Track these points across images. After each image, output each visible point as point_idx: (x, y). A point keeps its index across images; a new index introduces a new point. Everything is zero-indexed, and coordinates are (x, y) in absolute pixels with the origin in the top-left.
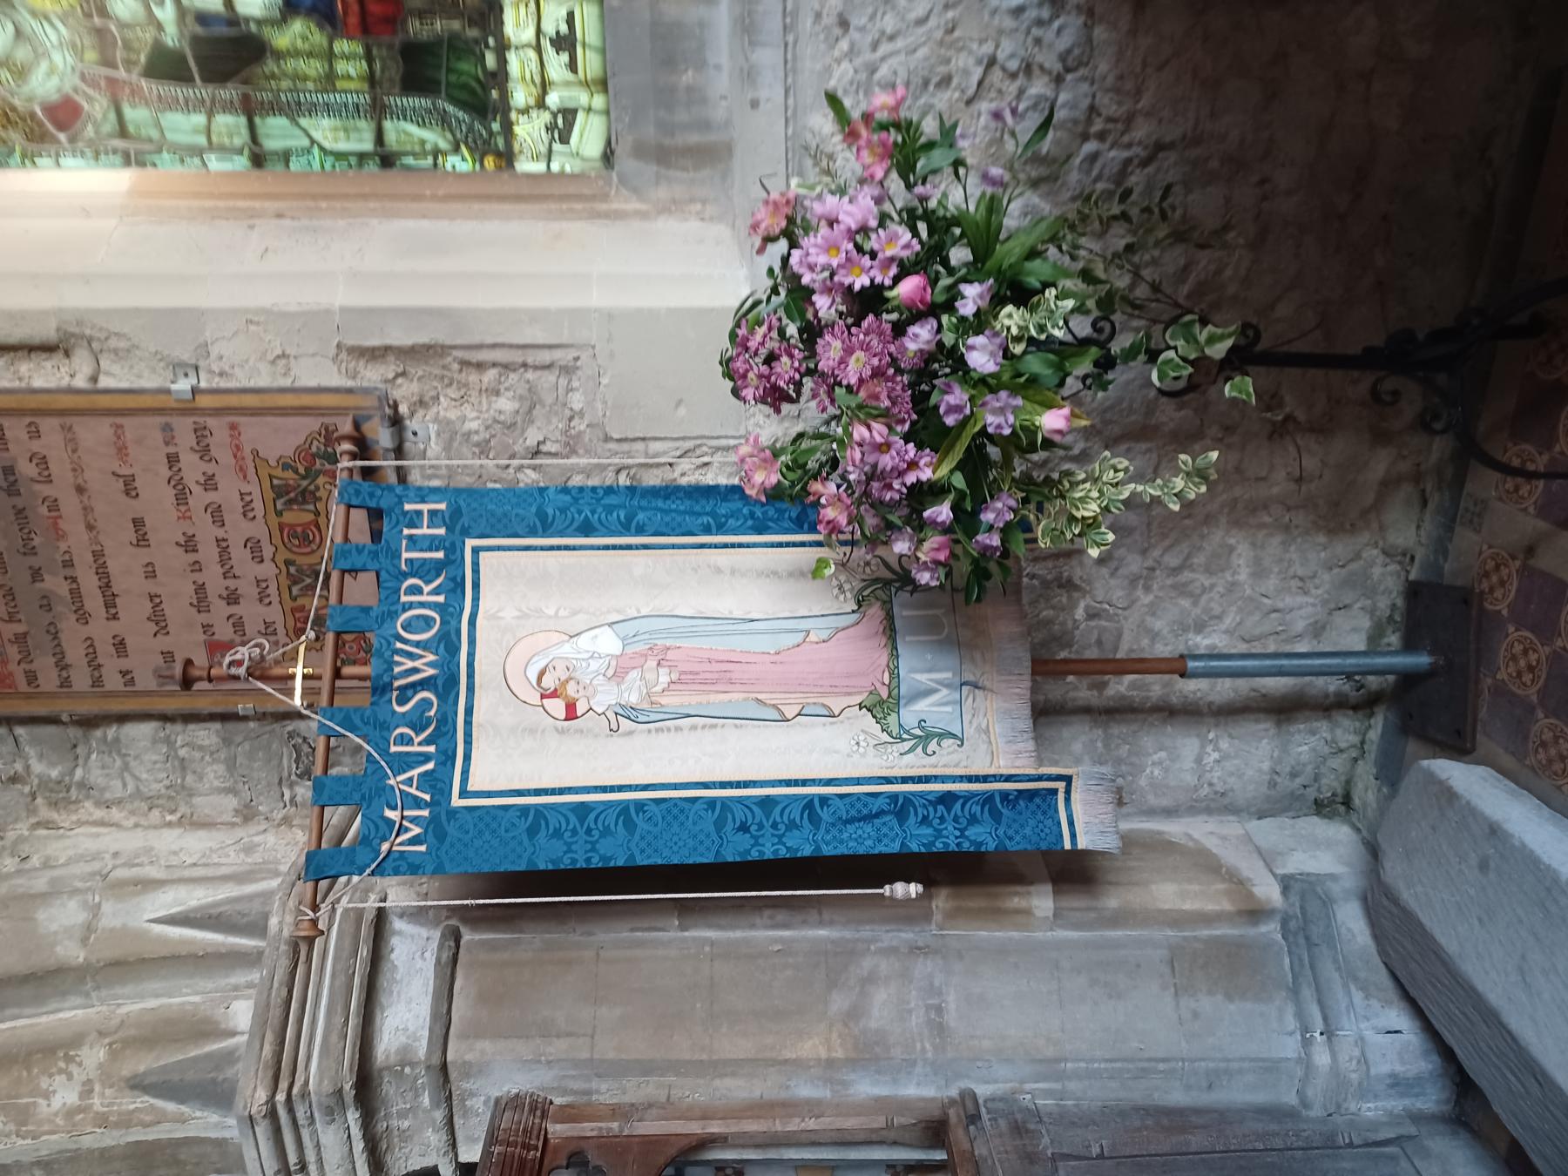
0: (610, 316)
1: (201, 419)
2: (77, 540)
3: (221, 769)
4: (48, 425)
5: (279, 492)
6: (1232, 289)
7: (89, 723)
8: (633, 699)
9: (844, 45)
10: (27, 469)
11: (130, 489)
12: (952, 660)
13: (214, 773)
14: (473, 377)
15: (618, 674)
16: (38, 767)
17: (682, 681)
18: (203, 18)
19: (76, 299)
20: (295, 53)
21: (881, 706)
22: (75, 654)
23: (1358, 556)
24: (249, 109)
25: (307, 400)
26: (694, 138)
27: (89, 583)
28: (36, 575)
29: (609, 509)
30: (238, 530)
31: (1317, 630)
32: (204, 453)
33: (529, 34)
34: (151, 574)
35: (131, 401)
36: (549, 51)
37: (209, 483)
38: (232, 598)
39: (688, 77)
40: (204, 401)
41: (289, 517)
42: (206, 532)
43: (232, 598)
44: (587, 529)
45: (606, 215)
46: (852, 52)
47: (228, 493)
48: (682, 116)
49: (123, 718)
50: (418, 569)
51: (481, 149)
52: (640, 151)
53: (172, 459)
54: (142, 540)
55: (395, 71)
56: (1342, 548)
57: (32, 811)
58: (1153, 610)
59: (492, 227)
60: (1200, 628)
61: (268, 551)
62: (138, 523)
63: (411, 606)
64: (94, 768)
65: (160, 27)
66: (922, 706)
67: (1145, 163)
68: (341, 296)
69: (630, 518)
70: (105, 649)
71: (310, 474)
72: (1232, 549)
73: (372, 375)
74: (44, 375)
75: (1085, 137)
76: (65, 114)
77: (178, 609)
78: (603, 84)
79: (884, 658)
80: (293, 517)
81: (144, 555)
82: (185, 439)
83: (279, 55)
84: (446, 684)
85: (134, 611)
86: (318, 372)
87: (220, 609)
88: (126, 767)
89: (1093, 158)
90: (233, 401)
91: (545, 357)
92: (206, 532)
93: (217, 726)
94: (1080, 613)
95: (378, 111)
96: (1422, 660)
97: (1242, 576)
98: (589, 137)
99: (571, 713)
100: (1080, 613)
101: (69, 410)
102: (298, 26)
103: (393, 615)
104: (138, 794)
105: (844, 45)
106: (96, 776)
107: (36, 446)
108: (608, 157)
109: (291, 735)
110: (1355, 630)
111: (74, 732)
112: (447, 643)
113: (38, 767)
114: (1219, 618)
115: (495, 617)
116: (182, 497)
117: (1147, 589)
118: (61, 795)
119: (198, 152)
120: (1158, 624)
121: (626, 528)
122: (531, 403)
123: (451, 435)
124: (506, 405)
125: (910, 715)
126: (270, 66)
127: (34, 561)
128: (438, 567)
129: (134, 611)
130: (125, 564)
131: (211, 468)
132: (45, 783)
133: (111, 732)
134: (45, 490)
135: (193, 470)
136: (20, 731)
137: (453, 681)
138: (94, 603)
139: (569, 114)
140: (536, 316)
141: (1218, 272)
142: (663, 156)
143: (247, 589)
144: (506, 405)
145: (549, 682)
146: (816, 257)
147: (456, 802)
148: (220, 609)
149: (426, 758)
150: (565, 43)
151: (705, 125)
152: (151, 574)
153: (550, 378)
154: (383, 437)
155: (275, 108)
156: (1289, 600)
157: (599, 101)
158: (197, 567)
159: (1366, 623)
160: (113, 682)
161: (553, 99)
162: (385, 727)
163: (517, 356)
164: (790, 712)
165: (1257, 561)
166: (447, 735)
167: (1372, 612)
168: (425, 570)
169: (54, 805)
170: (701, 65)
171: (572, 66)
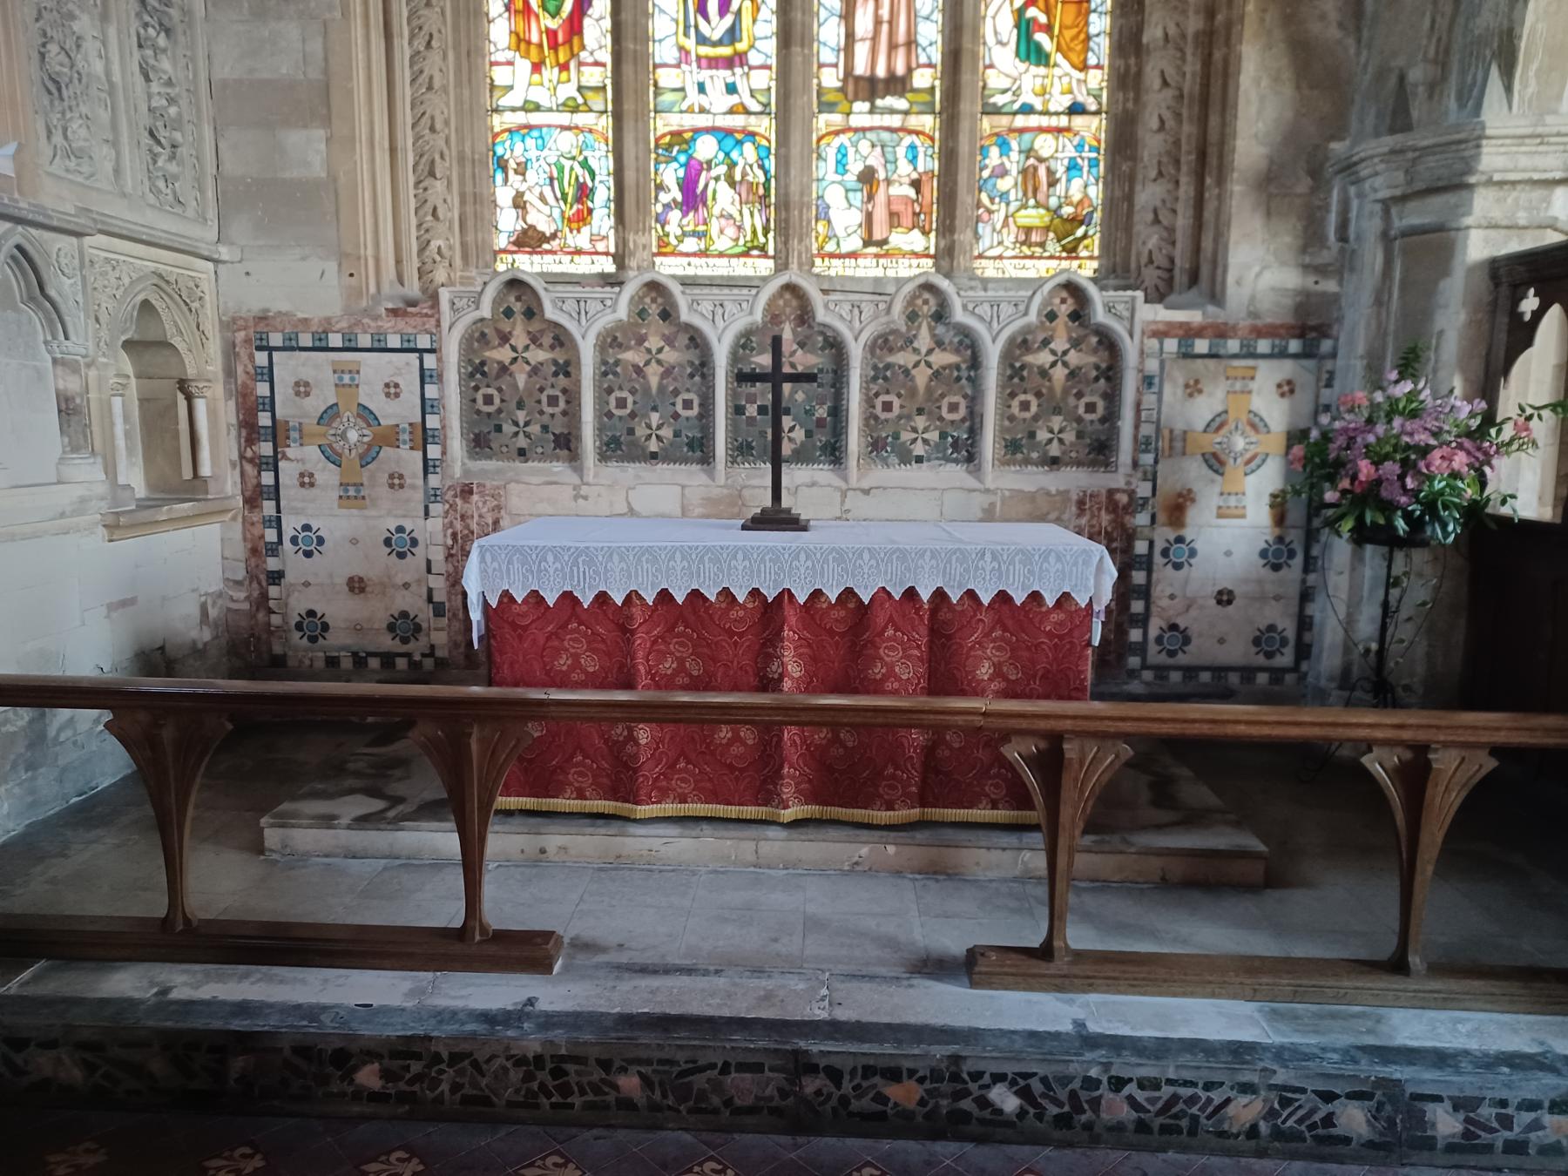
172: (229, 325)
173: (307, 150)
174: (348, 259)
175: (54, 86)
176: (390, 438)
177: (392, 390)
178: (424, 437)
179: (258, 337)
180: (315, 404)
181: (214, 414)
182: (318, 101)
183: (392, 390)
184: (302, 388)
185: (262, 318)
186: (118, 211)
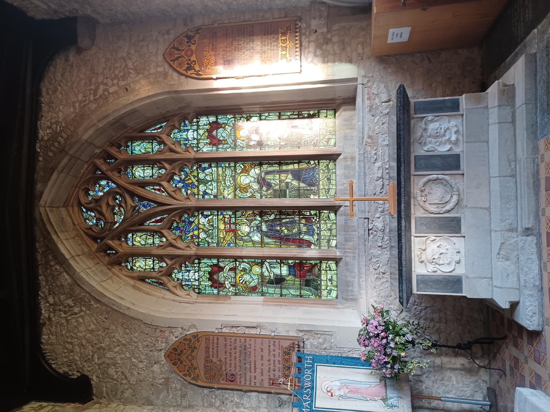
0: (338, 327)
1: (275, 339)
2: (252, 359)
3: (266, 403)
4: (253, 339)
5: (285, 352)
6: (443, 330)
7: (246, 392)
8: (342, 394)
9: (375, 290)
10: (248, 346)
11: (262, 351)
12: (396, 392)
13: (264, 404)
14: (316, 336)
15: (340, 389)
16: (236, 399)
17: (351, 391)
18: (277, 275)
19: (260, 320)
20: (290, 281)
21: (384, 400)
22: (248, 379)
23: (477, 381)
24: (281, 288)
25: (291, 338)
26: (351, 297)
27: (253, 366)
28: (245, 364)
29: (338, 360)
30: (277, 358)
31: (472, 396)
32: (274, 345)
33: (325, 279)
34: (262, 365)
35: (265, 336)
36: (328, 281)
37: (274, 350)
38: (274, 371)
39: (351, 288)
40: (276, 337)
41: (285, 357)
42: (272, 358)
43: (274, 371)
44: (334, 363)
45: (337, 308)
46: (376, 292)
47: (276, 353)
48: (349, 294)
49: (252, 391)
50: (307, 368)
51: (316, 296)
52: (343, 298)
53: (269, 346)
54: (262, 359)
55: (304, 283)
56: (473, 379)
57: (233, 408)
58: (438, 388)
59: (318, 309)
60: (448, 393)
61: (281, 362)
62: (262, 356)
63: (306, 374)
64: (245, 401)
65: (270, 276)
66: (391, 400)
67: (425, 310)
68: (298, 322)
69: (341, 362)
70: (253, 378)
71: (290, 350)
72: (451, 377)
73: (301, 334)
74: (253, 331)
75: (414, 305)
76: (254, 289)
77: (265, 372)
78: (337, 286)
79: (384, 391)
80: (286, 357)
81: (262, 362)
82: (272, 343)
83: (287, 281)
84: (312, 388)
85: (259, 371)
86: (293, 334)
87: (272, 372)
88: (250, 401)
89: (416, 308)
90: (280, 337)
91: (328, 333)
92: (272, 358)
93: (266, 394)
94: (424, 387)
95: (301, 289)
96: (489, 403)
97: (455, 383)
98: (334, 294)
99: (332, 396)
100: (424, 387)
102: (290, 277)
103: (304, 375)
104: (251, 407)
105: (375, 290)
106: (245, 403)
107: (250, 343)
108: (337, 297)
109: (279, 398)
110: (480, 397)
111: (243, 393)
112: (312, 381)
113: (236, 399)
114: (451, 391)
115: (319, 377)
116: (269, 353)
117: (436, 384)
118: (238, 405)
119: (273, 294)
120: (440, 391)
121: (341, 364)
122: (325, 340)
123: (312, 344)
124: (321, 340)
125: (389, 402)
126: (285, 282)
127: (245, 361)
128: (311, 368)
129: (259, 371)
130: (259, 363)
131: (275, 348)
132: (236, 402)
133: (249, 394)
134: (250, 350)
135: (272, 347)
136: (235, 392)
137: (313, 388)
138: (253, 370)
139: (331, 290)
140: (327, 327)
141: (440, 327)
142: (346, 300)
143: (277, 369)
144: (321, 340)
145: (329, 390)
146: (370, 328)
147: (314, 409)
148: (272, 372)
149: (309, 401)
150: (331, 280)
151: (353, 295)
152: (262, 365)
153: (328, 336)
154: (302, 345)
155: (286, 288)
156: (465, 389)
157: (336, 289)
158: (270, 364)
159: (482, 395)
160: (253, 384)
161: (328, 288)
162: (303, 395)
163: (323, 333)
164: (369, 399)
165: (457, 380)
166: (312, 397)
167: (483, 393)
168: (308, 368)
169: (236, 407)
170: (353, 287)
171: (332, 283)
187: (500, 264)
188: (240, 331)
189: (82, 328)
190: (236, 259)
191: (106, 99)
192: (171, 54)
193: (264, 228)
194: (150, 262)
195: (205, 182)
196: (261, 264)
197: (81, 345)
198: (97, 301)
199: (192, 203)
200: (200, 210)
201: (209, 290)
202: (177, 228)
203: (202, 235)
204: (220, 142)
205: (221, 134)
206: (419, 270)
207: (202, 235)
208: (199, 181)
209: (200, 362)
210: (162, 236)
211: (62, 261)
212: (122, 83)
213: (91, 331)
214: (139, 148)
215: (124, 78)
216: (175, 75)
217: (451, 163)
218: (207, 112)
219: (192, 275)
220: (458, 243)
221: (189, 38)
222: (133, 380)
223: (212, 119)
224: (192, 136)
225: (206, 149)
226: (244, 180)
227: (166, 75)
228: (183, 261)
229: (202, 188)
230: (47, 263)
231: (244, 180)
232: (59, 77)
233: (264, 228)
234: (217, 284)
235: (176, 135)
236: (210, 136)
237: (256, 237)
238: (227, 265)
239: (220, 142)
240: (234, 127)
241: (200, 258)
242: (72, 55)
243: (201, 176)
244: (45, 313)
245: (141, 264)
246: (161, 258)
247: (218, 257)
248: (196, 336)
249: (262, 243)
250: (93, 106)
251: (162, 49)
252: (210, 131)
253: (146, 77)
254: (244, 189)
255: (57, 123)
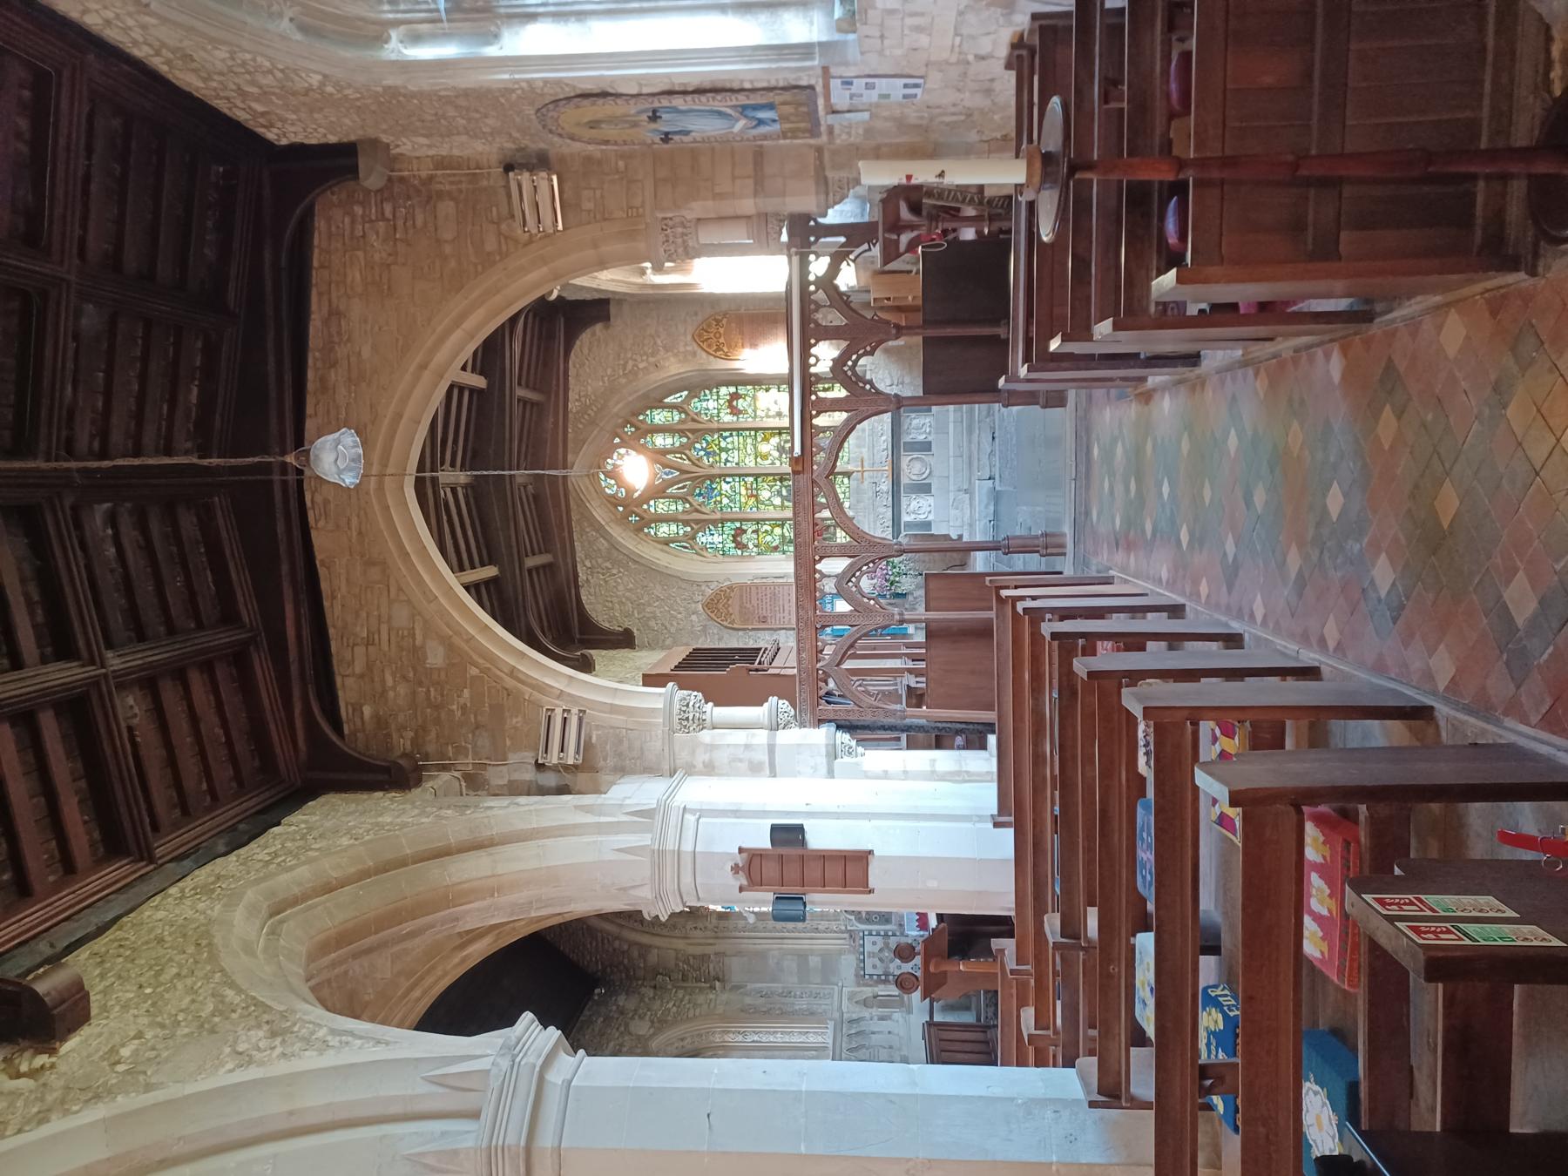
76: (776, 548)
101: (783, 585)
172: (859, 985)
173: (814, 961)
174: (841, 953)
175: (812, 1014)
176: (887, 945)
177: (874, 943)
178: (886, 935)
179: (861, 977)
180: (878, 963)
181: (882, 990)
182: (802, 957)
183: (874, 943)
184: (874, 967)
185: (857, 975)
186: (836, 1004)
187: (953, 512)
188: (770, 580)
189: (621, 588)
190: (758, 521)
191: (636, 374)
192: (700, 336)
193: (784, 493)
194: (673, 527)
195: (727, 450)
196: (782, 526)
197: (621, 603)
198: (635, 562)
199: (715, 471)
200: (722, 476)
201: (733, 551)
202: (700, 495)
203: (725, 501)
204: (740, 412)
205: (741, 404)
206: (905, 518)
207: (725, 501)
208: (722, 450)
209: (735, 609)
210: (685, 501)
211: (600, 529)
212: (652, 360)
213: (630, 590)
214: (660, 417)
215: (653, 355)
216: (704, 355)
217: (926, 447)
218: (727, 384)
219: (717, 539)
220: (931, 500)
221: (718, 322)
222: (673, 630)
223: (732, 389)
224: (711, 405)
225: (727, 418)
226: (764, 448)
227: (694, 354)
228: (703, 524)
229: (724, 456)
230: (583, 529)
231: (764, 448)
232: (586, 351)
233: (784, 493)
234: (740, 546)
235: (696, 405)
236: (731, 406)
237: (777, 501)
238: (750, 527)
239: (740, 412)
240: (754, 398)
241: (723, 521)
242: (598, 328)
243: (723, 444)
244: (582, 577)
245: (665, 530)
246: (686, 523)
247: (741, 521)
248: (731, 588)
249: (783, 507)
250: (623, 381)
251: (690, 330)
252: (730, 402)
253: (676, 355)
254: (765, 457)
255: (586, 396)
